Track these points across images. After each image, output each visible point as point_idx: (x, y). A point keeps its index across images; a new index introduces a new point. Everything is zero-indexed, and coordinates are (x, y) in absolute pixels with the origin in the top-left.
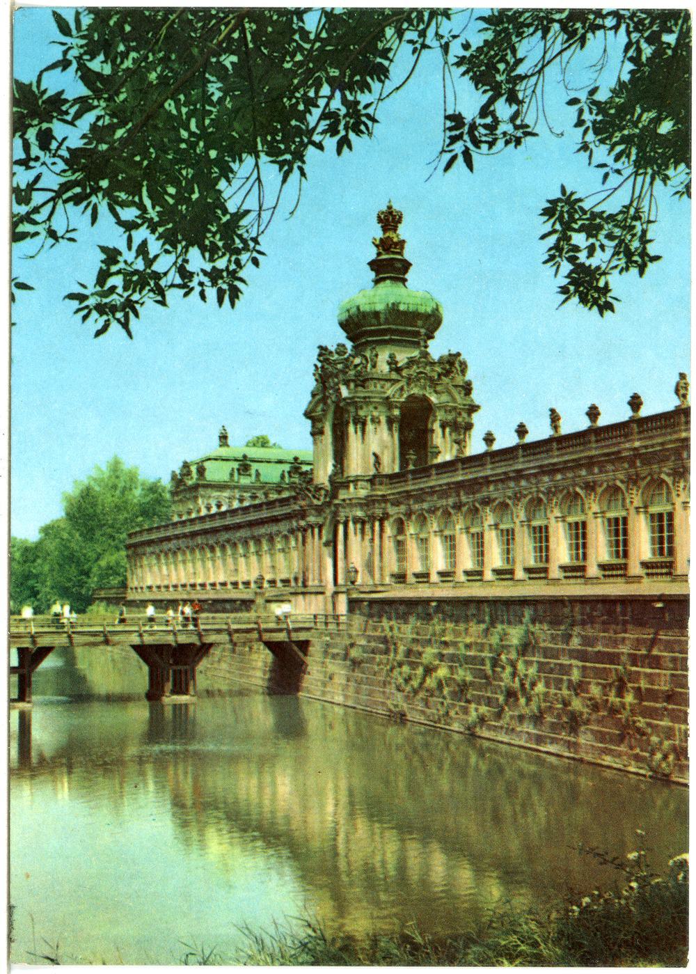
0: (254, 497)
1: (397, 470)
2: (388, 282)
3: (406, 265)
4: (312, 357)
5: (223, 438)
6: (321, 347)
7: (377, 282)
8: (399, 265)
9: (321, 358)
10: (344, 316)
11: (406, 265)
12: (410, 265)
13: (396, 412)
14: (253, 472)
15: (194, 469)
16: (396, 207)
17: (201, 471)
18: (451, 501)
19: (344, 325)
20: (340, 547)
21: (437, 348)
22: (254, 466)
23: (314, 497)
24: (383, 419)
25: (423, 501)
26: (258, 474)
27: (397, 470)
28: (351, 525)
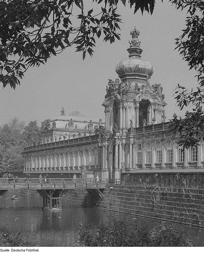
0: (79, 135)
1: (138, 127)
2: (134, 56)
3: (141, 51)
4: (106, 84)
5: (63, 112)
6: (110, 80)
7: (130, 56)
8: (138, 51)
9: (110, 84)
10: (118, 69)
11: (141, 51)
12: (142, 51)
13: (138, 105)
14: (74, 125)
15: (51, 123)
16: (137, 29)
17: (54, 125)
18: (160, 138)
19: (118, 72)
20: (117, 154)
21: (152, 81)
22: (75, 124)
23: (106, 135)
24: (133, 108)
25: (149, 138)
26: (76, 126)
27: (138, 127)
28: (120, 146)
